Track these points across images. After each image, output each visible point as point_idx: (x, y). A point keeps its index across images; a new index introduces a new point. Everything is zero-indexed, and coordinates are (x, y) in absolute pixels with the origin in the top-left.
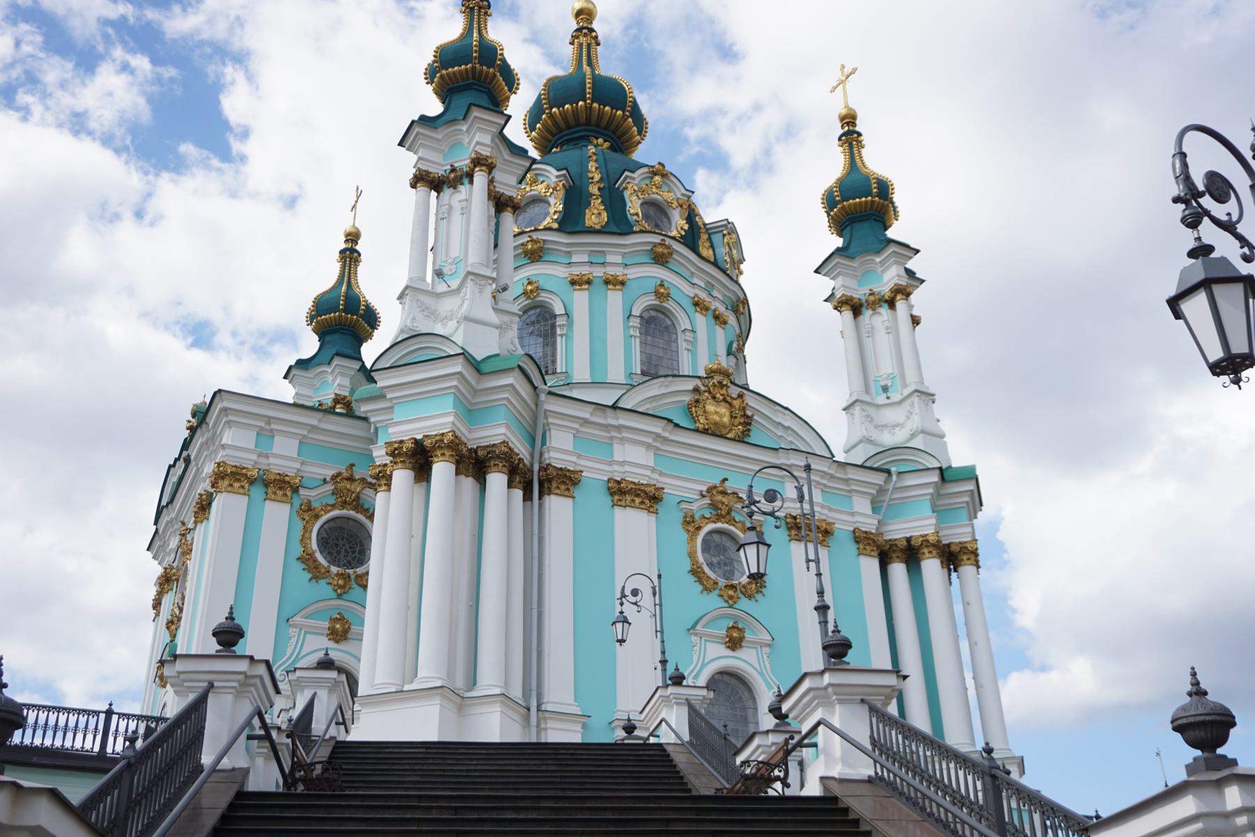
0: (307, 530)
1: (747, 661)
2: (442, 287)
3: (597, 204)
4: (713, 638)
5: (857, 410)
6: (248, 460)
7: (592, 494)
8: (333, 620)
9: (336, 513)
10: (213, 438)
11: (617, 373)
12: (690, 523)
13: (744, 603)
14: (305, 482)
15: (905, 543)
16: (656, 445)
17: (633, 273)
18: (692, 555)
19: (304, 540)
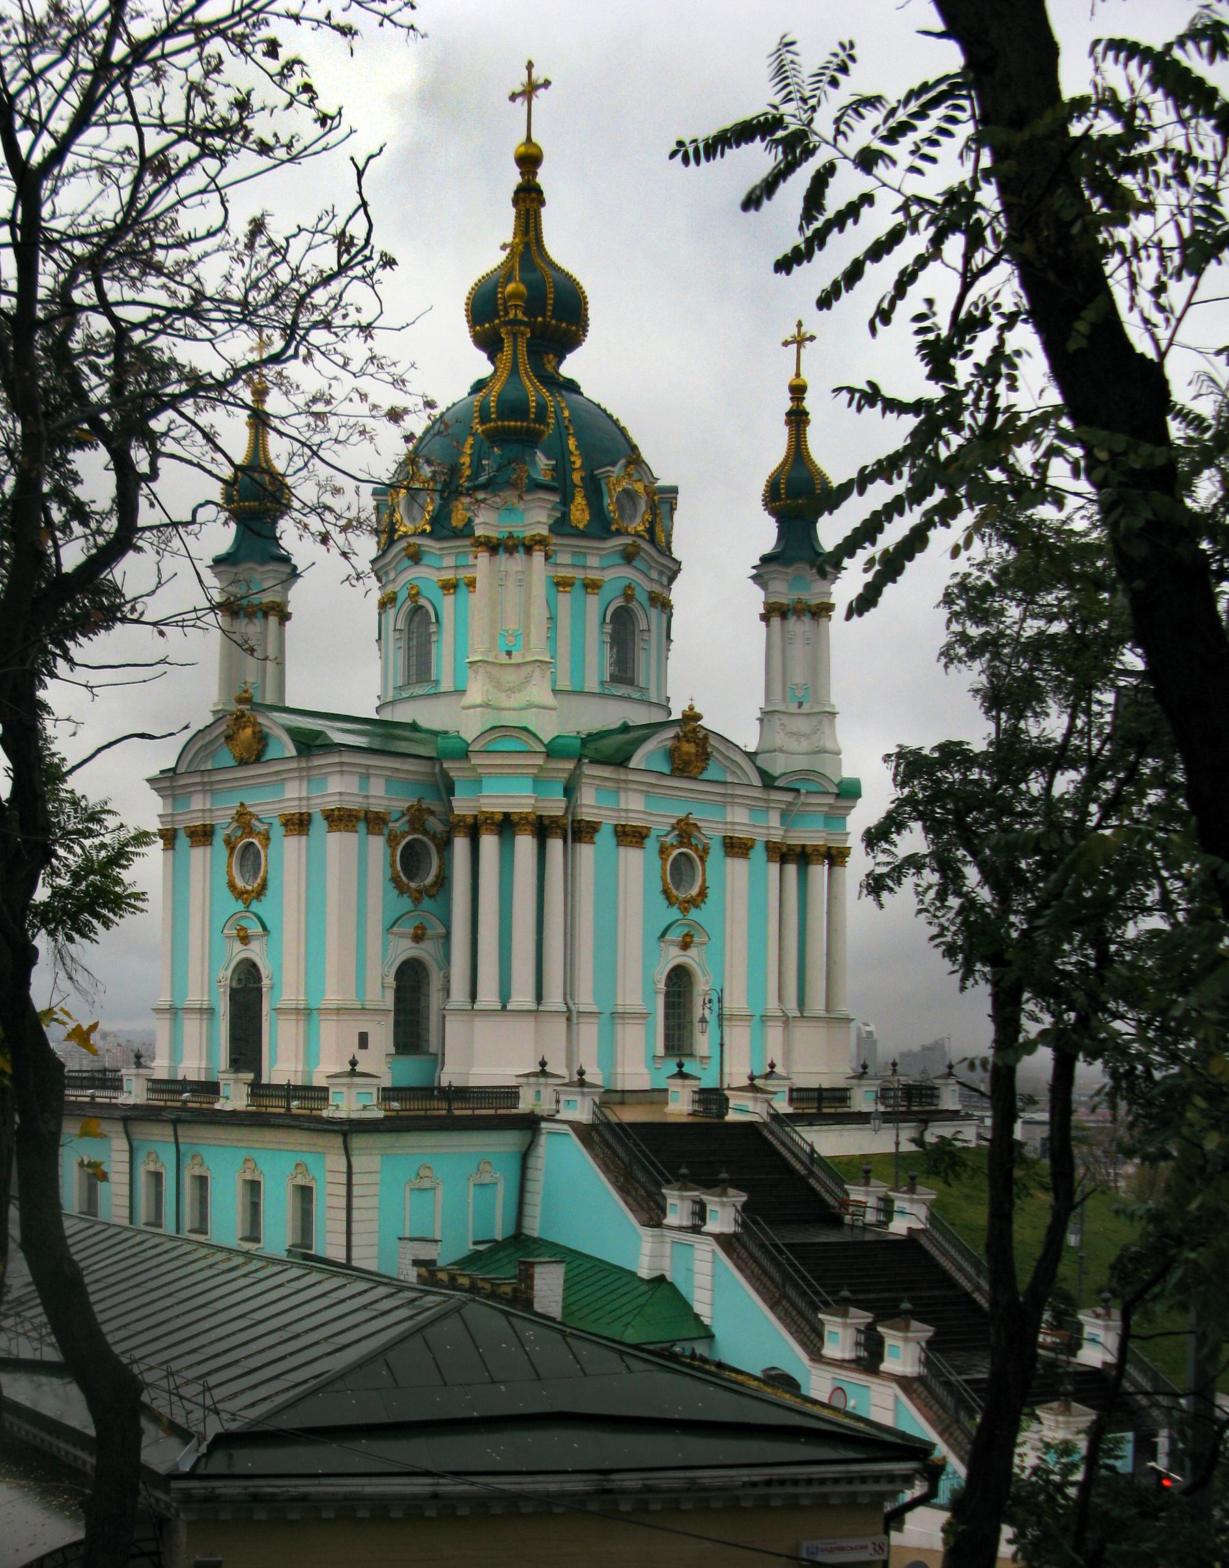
0: (393, 855)
1: (691, 958)
2: (504, 659)
3: (580, 500)
4: (673, 943)
5: (776, 718)
6: (354, 804)
7: (605, 837)
8: (417, 928)
9: (410, 837)
10: (309, 768)
11: (592, 685)
12: (663, 851)
13: (694, 914)
14: (394, 817)
15: (799, 850)
16: (648, 792)
17: (608, 575)
18: (663, 879)
19: (393, 865)
